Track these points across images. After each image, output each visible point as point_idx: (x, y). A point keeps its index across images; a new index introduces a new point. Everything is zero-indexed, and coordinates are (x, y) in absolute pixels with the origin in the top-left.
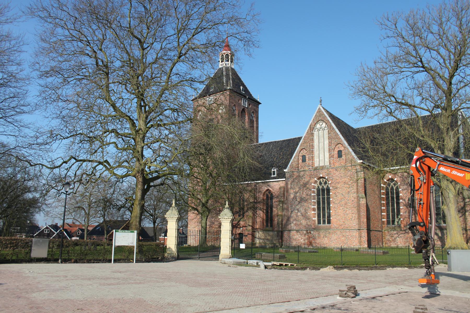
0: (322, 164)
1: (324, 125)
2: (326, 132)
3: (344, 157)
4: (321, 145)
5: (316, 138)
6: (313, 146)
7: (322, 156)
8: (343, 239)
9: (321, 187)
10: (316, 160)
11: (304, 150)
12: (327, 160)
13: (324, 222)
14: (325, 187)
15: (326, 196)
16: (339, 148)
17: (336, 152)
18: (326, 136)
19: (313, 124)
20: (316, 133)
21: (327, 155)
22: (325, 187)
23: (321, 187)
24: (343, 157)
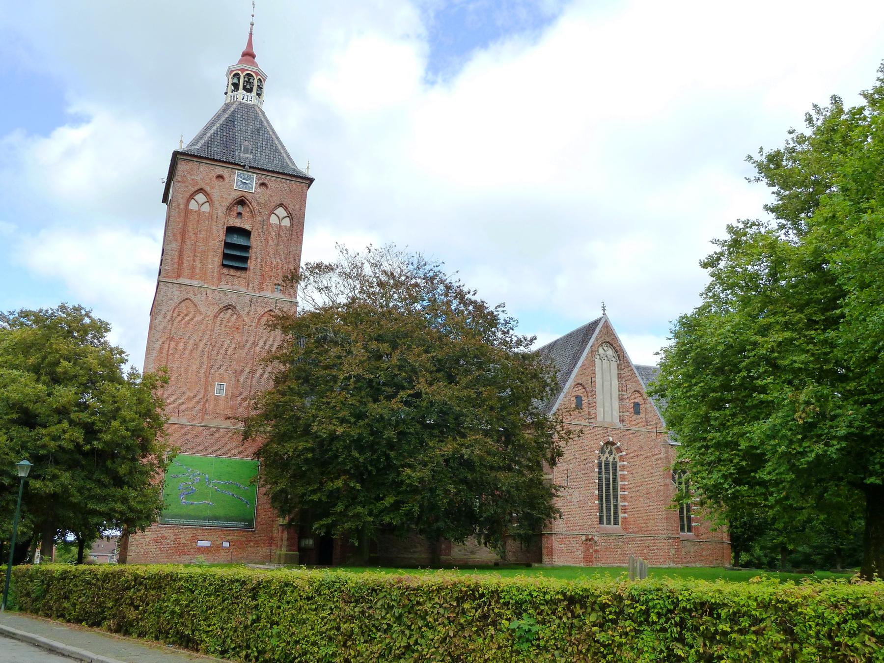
0: (608, 419)
1: (610, 352)
2: (614, 365)
3: (642, 415)
4: (607, 384)
5: (598, 369)
6: (593, 383)
7: (607, 404)
8: (645, 551)
9: (603, 459)
10: (600, 410)
11: (580, 387)
12: (616, 414)
13: (609, 520)
14: (611, 459)
15: (604, 476)
16: (635, 398)
17: (629, 405)
18: (615, 372)
19: (597, 345)
20: (597, 361)
21: (616, 405)
22: (611, 459)
23: (603, 459)
24: (641, 415)
